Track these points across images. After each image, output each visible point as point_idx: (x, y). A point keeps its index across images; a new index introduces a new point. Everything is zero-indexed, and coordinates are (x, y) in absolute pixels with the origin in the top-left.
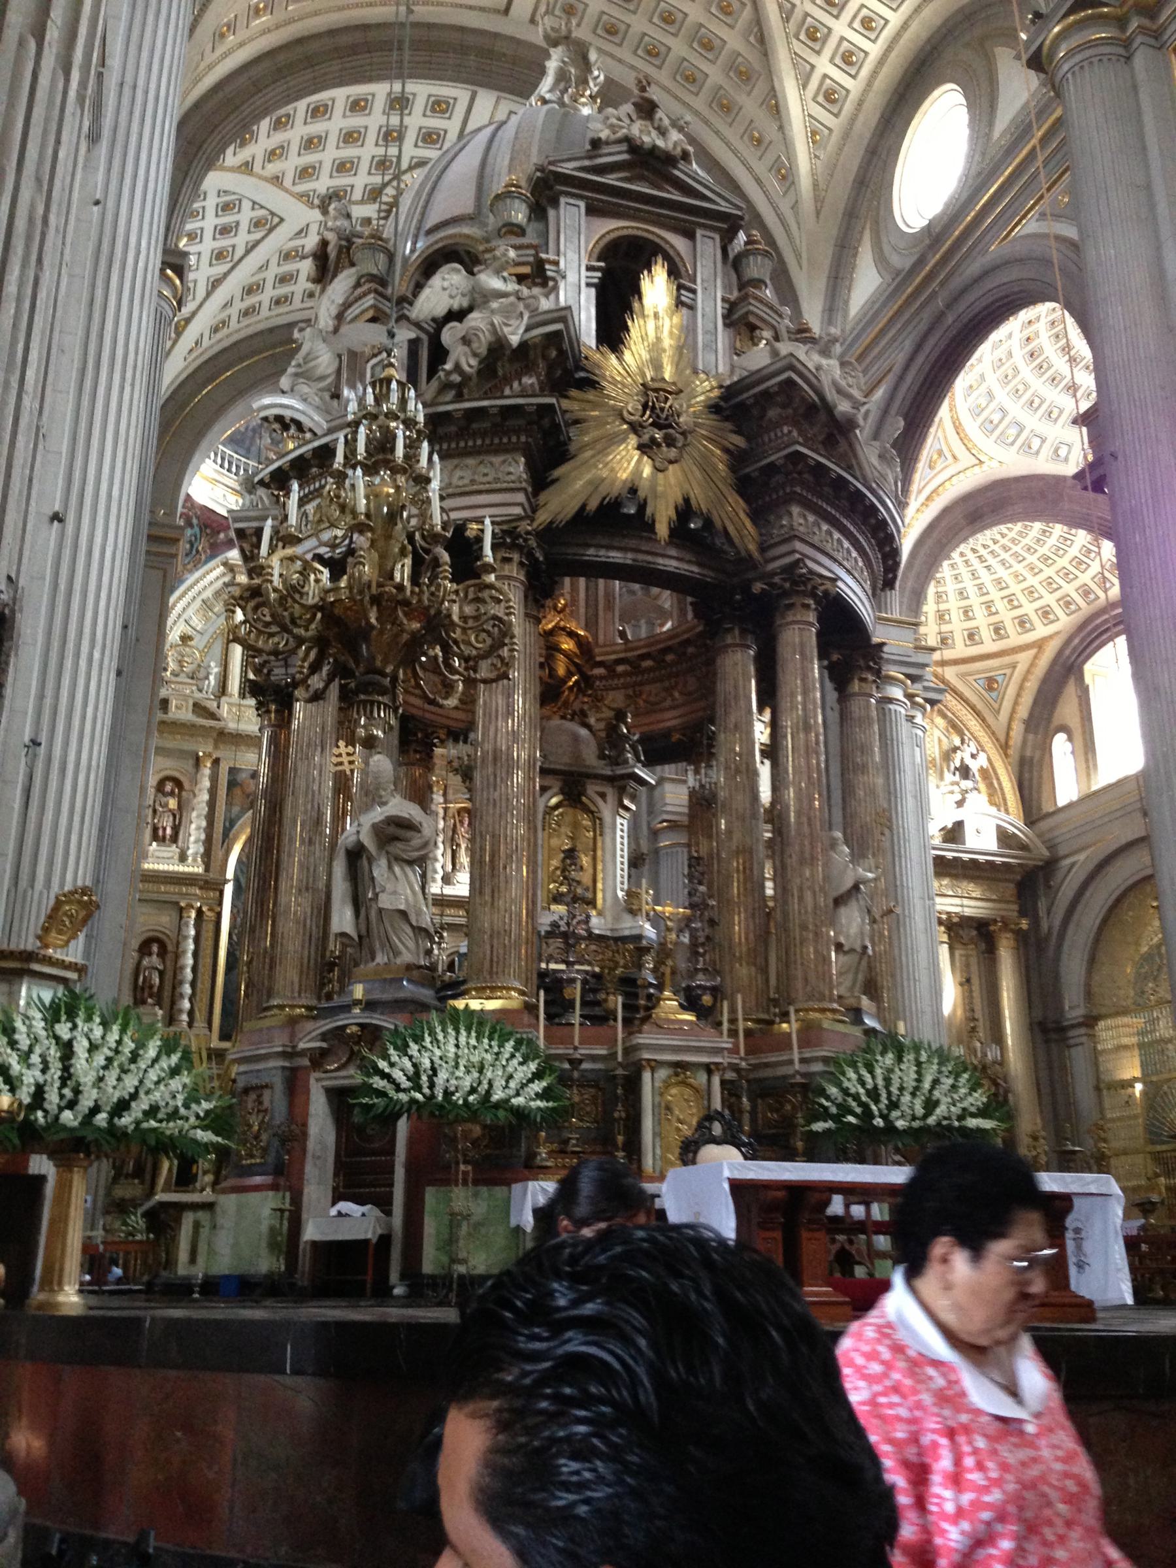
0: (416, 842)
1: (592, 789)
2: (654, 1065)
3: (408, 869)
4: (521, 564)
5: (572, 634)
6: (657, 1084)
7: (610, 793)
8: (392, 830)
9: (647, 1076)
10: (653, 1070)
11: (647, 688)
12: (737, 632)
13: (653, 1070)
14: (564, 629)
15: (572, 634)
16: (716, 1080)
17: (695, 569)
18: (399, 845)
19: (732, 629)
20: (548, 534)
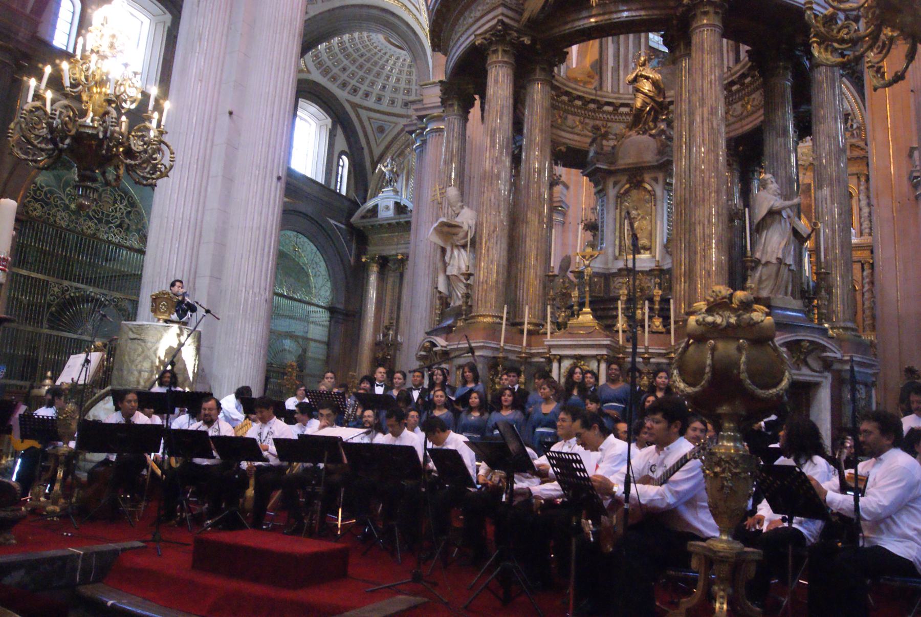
0: (461, 235)
1: (647, 177)
2: (560, 359)
3: (462, 250)
4: (504, 51)
5: (647, 78)
6: (562, 371)
7: (661, 176)
8: (446, 229)
9: (555, 365)
10: (560, 362)
11: (753, 96)
12: (682, 46)
13: (560, 362)
14: (642, 76)
15: (647, 78)
16: (603, 366)
17: (643, 13)
18: (455, 238)
19: (679, 45)
20: (533, 25)
